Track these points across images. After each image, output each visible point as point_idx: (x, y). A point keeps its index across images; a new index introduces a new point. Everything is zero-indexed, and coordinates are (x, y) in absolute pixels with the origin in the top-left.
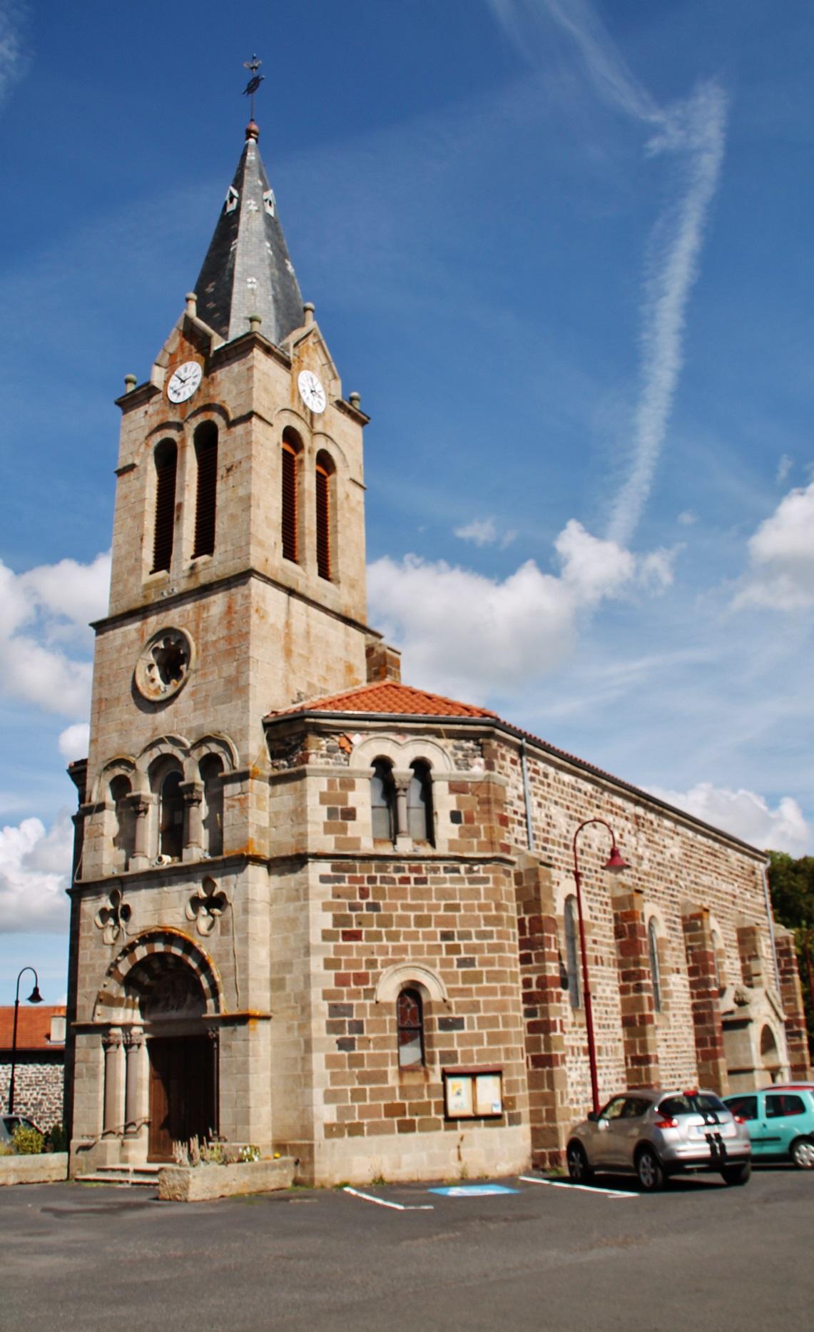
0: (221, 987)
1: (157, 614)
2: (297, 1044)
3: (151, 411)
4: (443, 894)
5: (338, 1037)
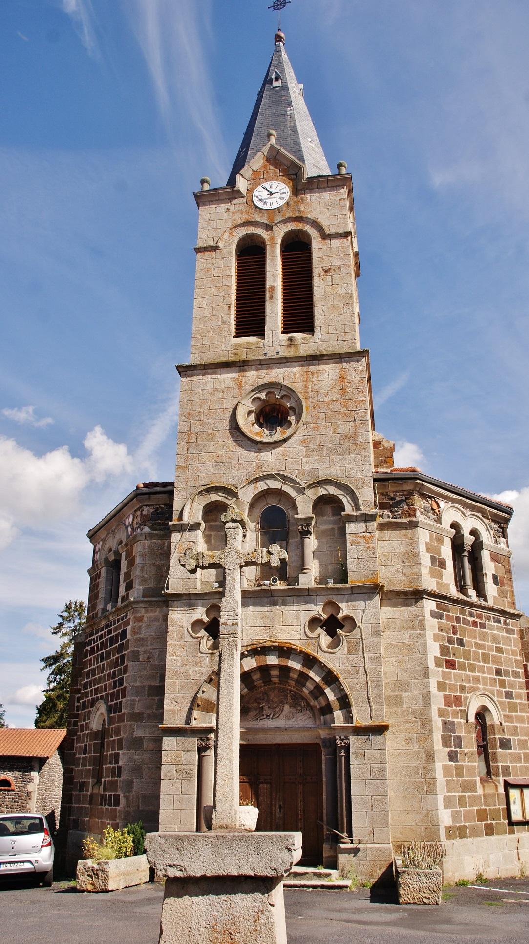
0: (352, 700)
1: (258, 369)
2: (417, 755)
3: (233, 208)
4: (495, 639)
5: (449, 749)
